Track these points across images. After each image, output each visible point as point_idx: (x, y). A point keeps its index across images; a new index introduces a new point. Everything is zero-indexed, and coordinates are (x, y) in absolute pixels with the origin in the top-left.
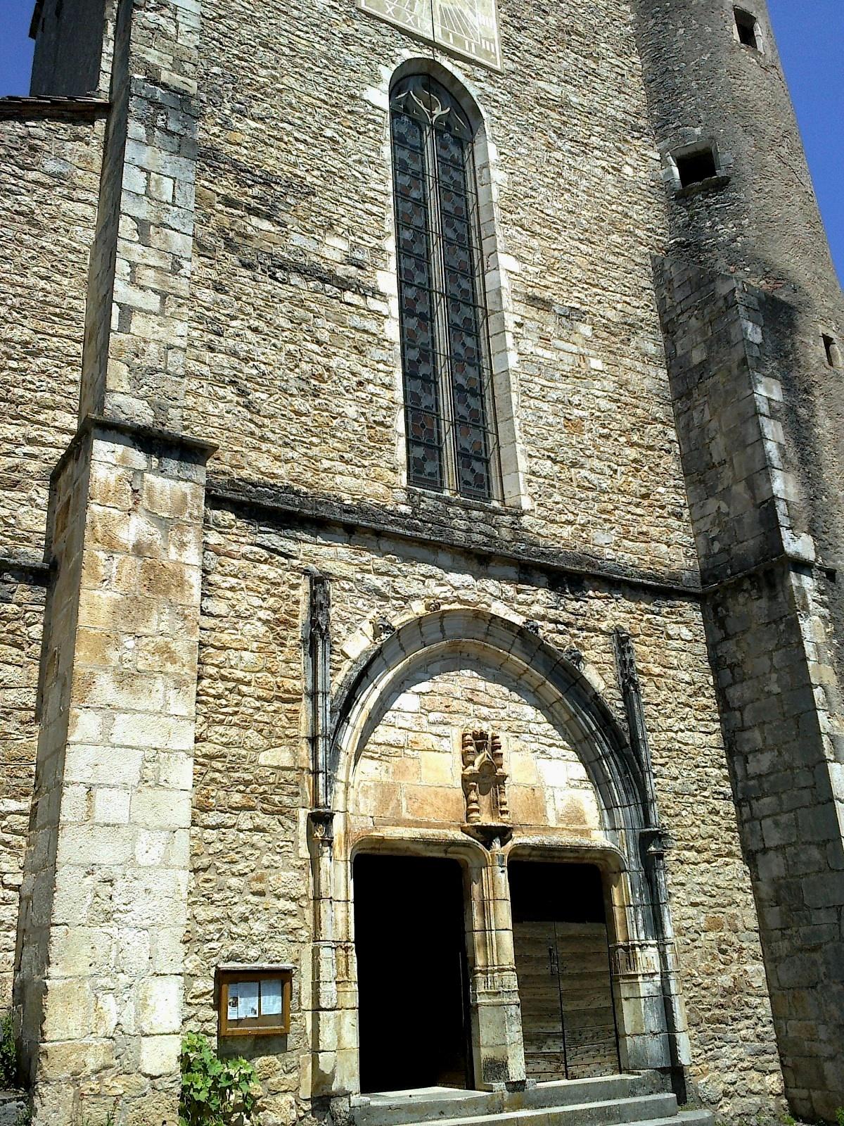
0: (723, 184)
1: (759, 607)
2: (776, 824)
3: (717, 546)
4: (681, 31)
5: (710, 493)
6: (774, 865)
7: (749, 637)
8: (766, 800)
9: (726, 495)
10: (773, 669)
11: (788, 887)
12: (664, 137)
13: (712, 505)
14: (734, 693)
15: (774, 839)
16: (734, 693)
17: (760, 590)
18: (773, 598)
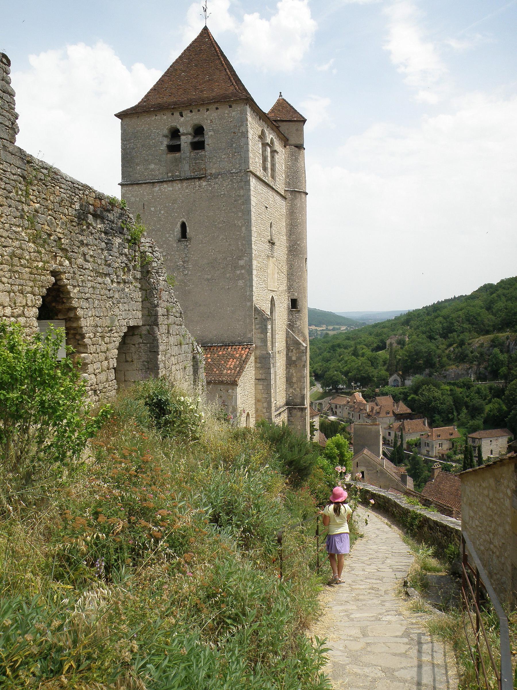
0: (299, 311)
1: (299, 414)
3: (291, 398)
5: (292, 387)
9: (295, 389)
13: (291, 390)
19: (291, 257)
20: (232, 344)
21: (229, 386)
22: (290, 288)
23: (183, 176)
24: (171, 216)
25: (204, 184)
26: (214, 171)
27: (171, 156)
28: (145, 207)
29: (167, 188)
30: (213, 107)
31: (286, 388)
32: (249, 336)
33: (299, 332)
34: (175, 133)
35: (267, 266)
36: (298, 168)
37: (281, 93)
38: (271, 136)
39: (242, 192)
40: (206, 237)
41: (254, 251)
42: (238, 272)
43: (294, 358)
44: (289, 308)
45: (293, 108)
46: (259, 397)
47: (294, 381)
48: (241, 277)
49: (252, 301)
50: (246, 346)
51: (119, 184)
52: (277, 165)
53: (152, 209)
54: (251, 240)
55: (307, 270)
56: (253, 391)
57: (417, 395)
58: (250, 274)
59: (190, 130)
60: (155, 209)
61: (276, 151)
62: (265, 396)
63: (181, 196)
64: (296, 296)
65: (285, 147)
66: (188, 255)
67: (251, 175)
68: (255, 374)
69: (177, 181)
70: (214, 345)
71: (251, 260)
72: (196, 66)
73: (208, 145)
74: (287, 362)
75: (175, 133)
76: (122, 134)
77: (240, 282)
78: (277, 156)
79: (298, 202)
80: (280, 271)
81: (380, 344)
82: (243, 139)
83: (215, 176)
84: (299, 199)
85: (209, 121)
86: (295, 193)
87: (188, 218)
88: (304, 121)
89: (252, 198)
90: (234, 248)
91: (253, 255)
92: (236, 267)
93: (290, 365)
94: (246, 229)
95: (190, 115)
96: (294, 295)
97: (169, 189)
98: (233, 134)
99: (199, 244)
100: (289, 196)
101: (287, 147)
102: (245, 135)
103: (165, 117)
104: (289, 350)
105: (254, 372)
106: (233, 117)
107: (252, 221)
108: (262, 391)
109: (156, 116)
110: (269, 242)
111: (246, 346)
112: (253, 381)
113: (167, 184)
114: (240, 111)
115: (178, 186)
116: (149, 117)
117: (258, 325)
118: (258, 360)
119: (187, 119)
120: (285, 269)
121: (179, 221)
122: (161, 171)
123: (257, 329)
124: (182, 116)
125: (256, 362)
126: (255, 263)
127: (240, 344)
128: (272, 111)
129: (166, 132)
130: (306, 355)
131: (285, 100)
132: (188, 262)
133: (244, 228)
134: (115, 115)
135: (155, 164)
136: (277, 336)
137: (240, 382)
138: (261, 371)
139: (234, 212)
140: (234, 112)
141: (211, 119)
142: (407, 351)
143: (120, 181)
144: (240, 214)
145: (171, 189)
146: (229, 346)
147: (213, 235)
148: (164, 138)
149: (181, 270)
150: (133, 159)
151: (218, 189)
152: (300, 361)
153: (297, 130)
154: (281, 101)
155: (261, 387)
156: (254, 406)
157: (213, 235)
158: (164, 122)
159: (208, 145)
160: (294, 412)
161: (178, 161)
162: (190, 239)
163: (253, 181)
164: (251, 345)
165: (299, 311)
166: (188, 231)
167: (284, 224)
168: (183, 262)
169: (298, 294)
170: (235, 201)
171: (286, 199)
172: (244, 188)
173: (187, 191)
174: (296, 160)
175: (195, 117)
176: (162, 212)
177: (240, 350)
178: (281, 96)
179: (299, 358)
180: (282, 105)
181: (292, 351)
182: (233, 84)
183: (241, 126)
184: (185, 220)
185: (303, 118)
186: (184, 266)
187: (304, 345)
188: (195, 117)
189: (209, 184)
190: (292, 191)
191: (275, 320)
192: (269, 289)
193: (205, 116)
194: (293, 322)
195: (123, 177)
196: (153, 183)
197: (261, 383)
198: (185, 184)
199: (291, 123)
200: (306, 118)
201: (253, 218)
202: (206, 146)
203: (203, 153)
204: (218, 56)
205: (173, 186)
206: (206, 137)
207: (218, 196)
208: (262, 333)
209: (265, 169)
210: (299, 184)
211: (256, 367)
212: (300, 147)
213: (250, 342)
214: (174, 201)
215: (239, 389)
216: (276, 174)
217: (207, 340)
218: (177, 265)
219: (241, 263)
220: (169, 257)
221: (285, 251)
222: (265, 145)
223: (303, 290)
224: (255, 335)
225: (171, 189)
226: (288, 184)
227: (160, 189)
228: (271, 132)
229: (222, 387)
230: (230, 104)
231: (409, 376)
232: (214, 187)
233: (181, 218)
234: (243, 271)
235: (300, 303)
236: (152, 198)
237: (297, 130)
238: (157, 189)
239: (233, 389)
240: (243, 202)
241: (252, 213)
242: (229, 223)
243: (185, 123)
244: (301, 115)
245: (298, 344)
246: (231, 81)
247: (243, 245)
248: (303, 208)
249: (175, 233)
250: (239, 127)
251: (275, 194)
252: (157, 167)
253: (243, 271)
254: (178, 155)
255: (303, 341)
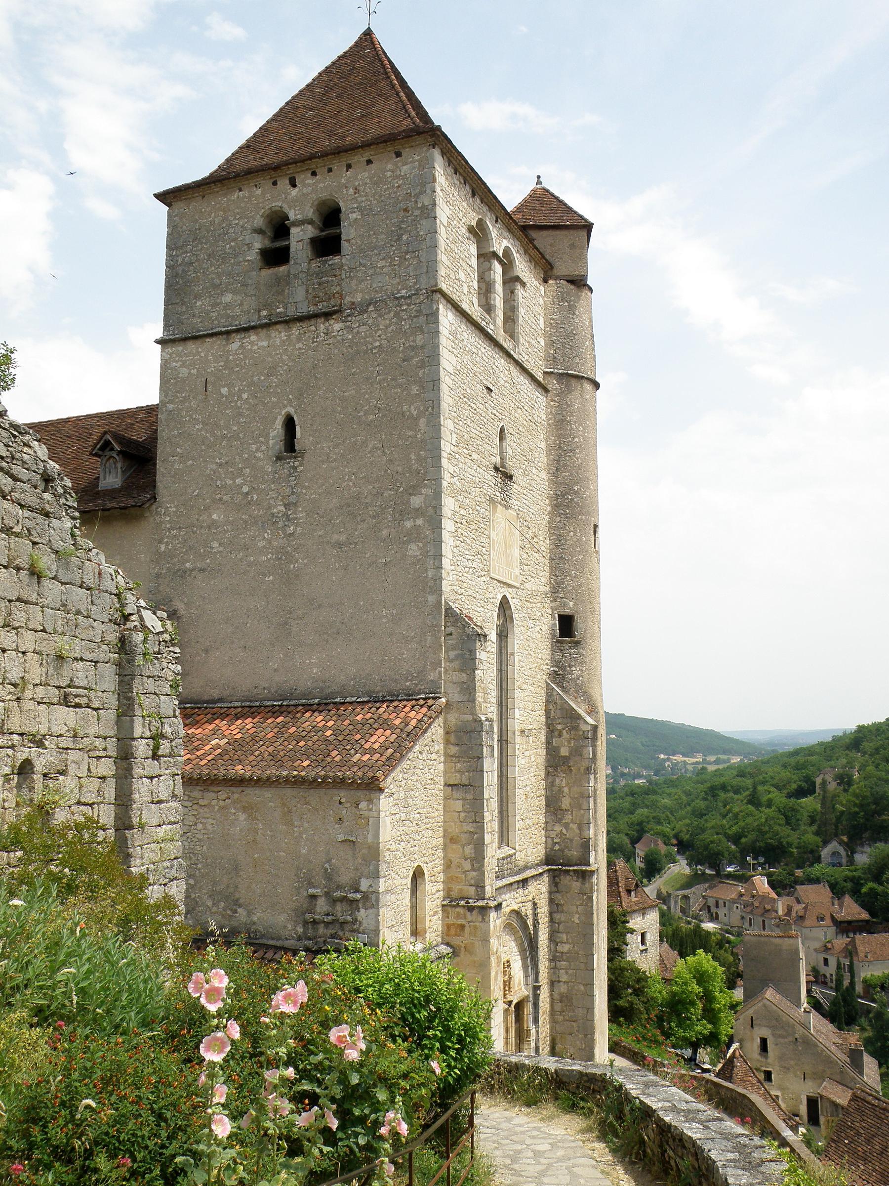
0: (578, 643)
1: (576, 885)
2: (567, 973)
3: (557, 847)
4: (572, 534)
5: (559, 821)
6: (563, 988)
7: (568, 895)
8: (564, 963)
9: (566, 826)
10: (577, 912)
11: (567, 997)
12: (555, 600)
13: (558, 828)
14: (557, 917)
15: (564, 978)
16: (557, 917)
17: (578, 877)
18: (583, 884)
19: (558, 519)
20: (391, 698)
21: (360, 794)
22: (556, 589)
23: (292, 312)
24: (263, 404)
25: (337, 326)
26: (358, 298)
27: (267, 273)
28: (210, 388)
29: (256, 342)
30: (358, 159)
31: (546, 823)
32: (432, 676)
33: (577, 692)
35: (487, 520)
36: (576, 328)
37: (539, 177)
38: (505, 243)
39: (419, 340)
40: (336, 446)
41: (446, 476)
42: (408, 524)
43: (564, 752)
44: (554, 636)
45: (565, 205)
46: (455, 830)
47: (564, 807)
48: (414, 535)
49: (438, 591)
50: (422, 702)
51: (158, 342)
52: (522, 311)
53: (224, 391)
54: (439, 449)
55: (597, 552)
56: (438, 814)
57: (881, 884)
58: (436, 526)
59: (310, 213)
60: (229, 391)
61: (517, 279)
62: (470, 828)
63: (285, 357)
64: (570, 607)
65: (545, 281)
66: (297, 490)
67: (442, 300)
68: (445, 772)
69: (278, 326)
70: (348, 699)
71: (437, 495)
72: (339, 96)
73: (348, 241)
74: (547, 760)
75: (280, 227)
76: (169, 235)
77: (413, 546)
78: (520, 292)
79: (575, 399)
80: (528, 545)
81: (804, 784)
82: (424, 222)
83: (362, 308)
84: (577, 393)
85: (351, 191)
86: (567, 378)
87: (300, 407)
88: (587, 227)
89: (444, 353)
90: (400, 469)
91: (445, 484)
92: (404, 512)
93: (555, 767)
94: (428, 422)
95: (310, 181)
96: (565, 605)
97: (260, 344)
98: (402, 213)
99: (323, 462)
100: (553, 384)
101: (551, 282)
102: (429, 213)
104: (552, 731)
105: (441, 767)
106: (404, 177)
107: (444, 406)
108: (463, 815)
109: (240, 190)
110: (496, 469)
111: (422, 702)
112: (438, 789)
113: (257, 334)
114: (420, 161)
115: (279, 335)
116: (225, 195)
117: (453, 649)
118: (453, 739)
119: (305, 191)
120: (544, 544)
121: (280, 414)
122: (246, 307)
123: (451, 661)
124: (294, 185)
125: (447, 742)
126: (449, 504)
127: (410, 696)
128: (519, 209)
129: (259, 221)
130: (594, 746)
131: (547, 191)
132: (295, 504)
133: (422, 422)
134: (155, 195)
135: (234, 292)
136: (518, 694)
137: (390, 783)
138: (459, 765)
139: (400, 386)
140: (407, 167)
141: (355, 187)
142: (856, 796)
143: (159, 333)
144: (415, 389)
145: (265, 344)
146: (383, 701)
147: (353, 440)
148: (256, 235)
149: (281, 524)
150: (190, 286)
151: (366, 337)
152: (577, 758)
153: (572, 246)
154: (539, 192)
155: (458, 805)
156: (440, 853)
157: (353, 440)
158: (257, 201)
159: (348, 241)
160: (565, 880)
161: (281, 283)
162: (303, 454)
163: (447, 319)
164: (435, 698)
165: (578, 643)
166: (298, 434)
167: (543, 445)
168: (285, 505)
169: (575, 604)
170: (404, 361)
171: (546, 390)
172: (426, 330)
173: (300, 345)
174: (572, 309)
175: (321, 185)
176: (245, 396)
177: (407, 709)
178: (539, 182)
179: (577, 752)
180: (542, 199)
181: (560, 736)
182: (409, 116)
183: (421, 193)
184: (292, 411)
185: (586, 220)
186: (288, 516)
187: (590, 720)
188: (321, 185)
189: (348, 327)
190: (562, 374)
191: (513, 654)
192: (492, 575)
193: (343, 181)
194: (563, 668)
195: (166, 326)
196: (228, 333)
197: (457, 794)
198: (295, 330)
199: (558, 232)
200: (591, 220)
201: (447, 399)
202: (344, 245)
203: (336, 259)
204: (386, 73)
205: (269, 337)
206: (344, 224)
207: (366, 352)
208: (462, 670)
209: (488, 308)
210: (577, 360)
211: (446, 755)
212: (579, 283)
213: (433, 693)
214: (272, 371)
215: (385, 803)
216: (520, 329)
217: (334, 688)
218: (273, 514)
219: (416, 501)
220: (255, 497)
221: (545, 505)
222: (486, 256)
223: (589, 596)
224: (446, 676)
225: (265, 344)
226: (552, 360)
227: (242, 346)
228: (506, 234)
229: (343, 794)
230: (398, 147)
231: (862, 845)
232: (358, 332)
233: (285, 406)
234: (420, 522)
235: (580, 626)
236: (225, 367)
237: (572, 246)
238: (235, 345)
239: (370, 801)
240: (422, 361)
241: (444, 388)
242: (390, 410)
243: (299, 200)
244: (581, 217)
245: (573, 717)
246: (406, 111)
247: (420, 459)
248: (588, 414)
249: (271, 442)
250: (417, 196)
251: (515, 372)
252: (238, 298)
253: (420, 522)
254: (282, 269)
255: (589, 714)
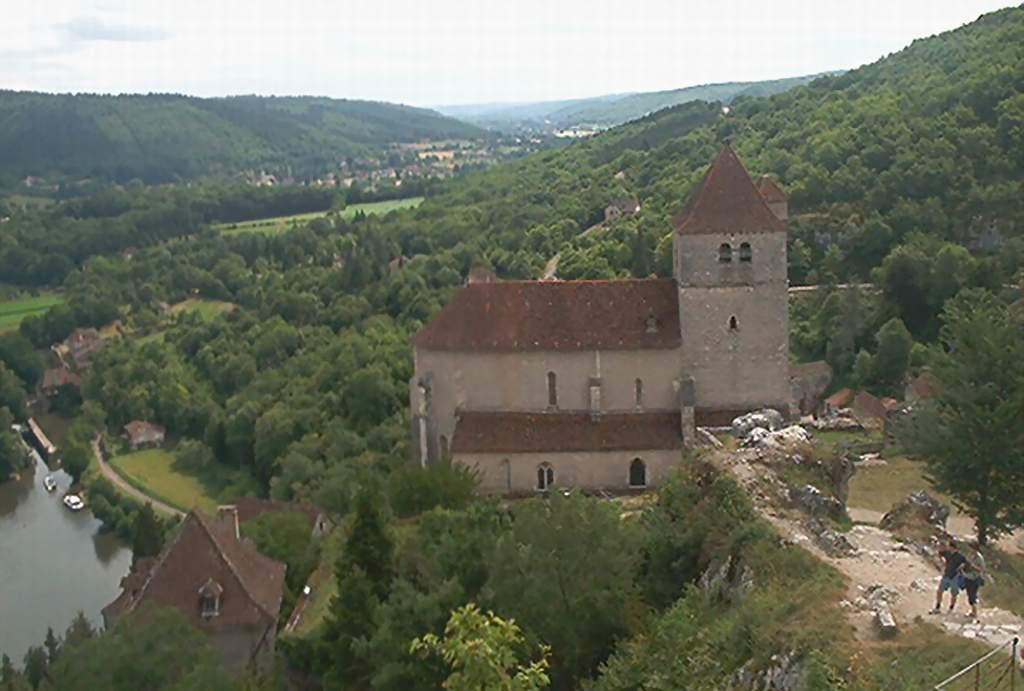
25: (751, 289)
27: (722, 266)
29: (720, 291)
34: (726, 247)
75: (726, 247)
83: (761, 283)
103: (719, 236)
115: (729, 290)
129: (719, 246)
161: (728, 272)
166: (738, 323)
198: (736, 289)
219: (780, 348)
238: (711, 291)
243: (735, 241)
254: (729, 265)
